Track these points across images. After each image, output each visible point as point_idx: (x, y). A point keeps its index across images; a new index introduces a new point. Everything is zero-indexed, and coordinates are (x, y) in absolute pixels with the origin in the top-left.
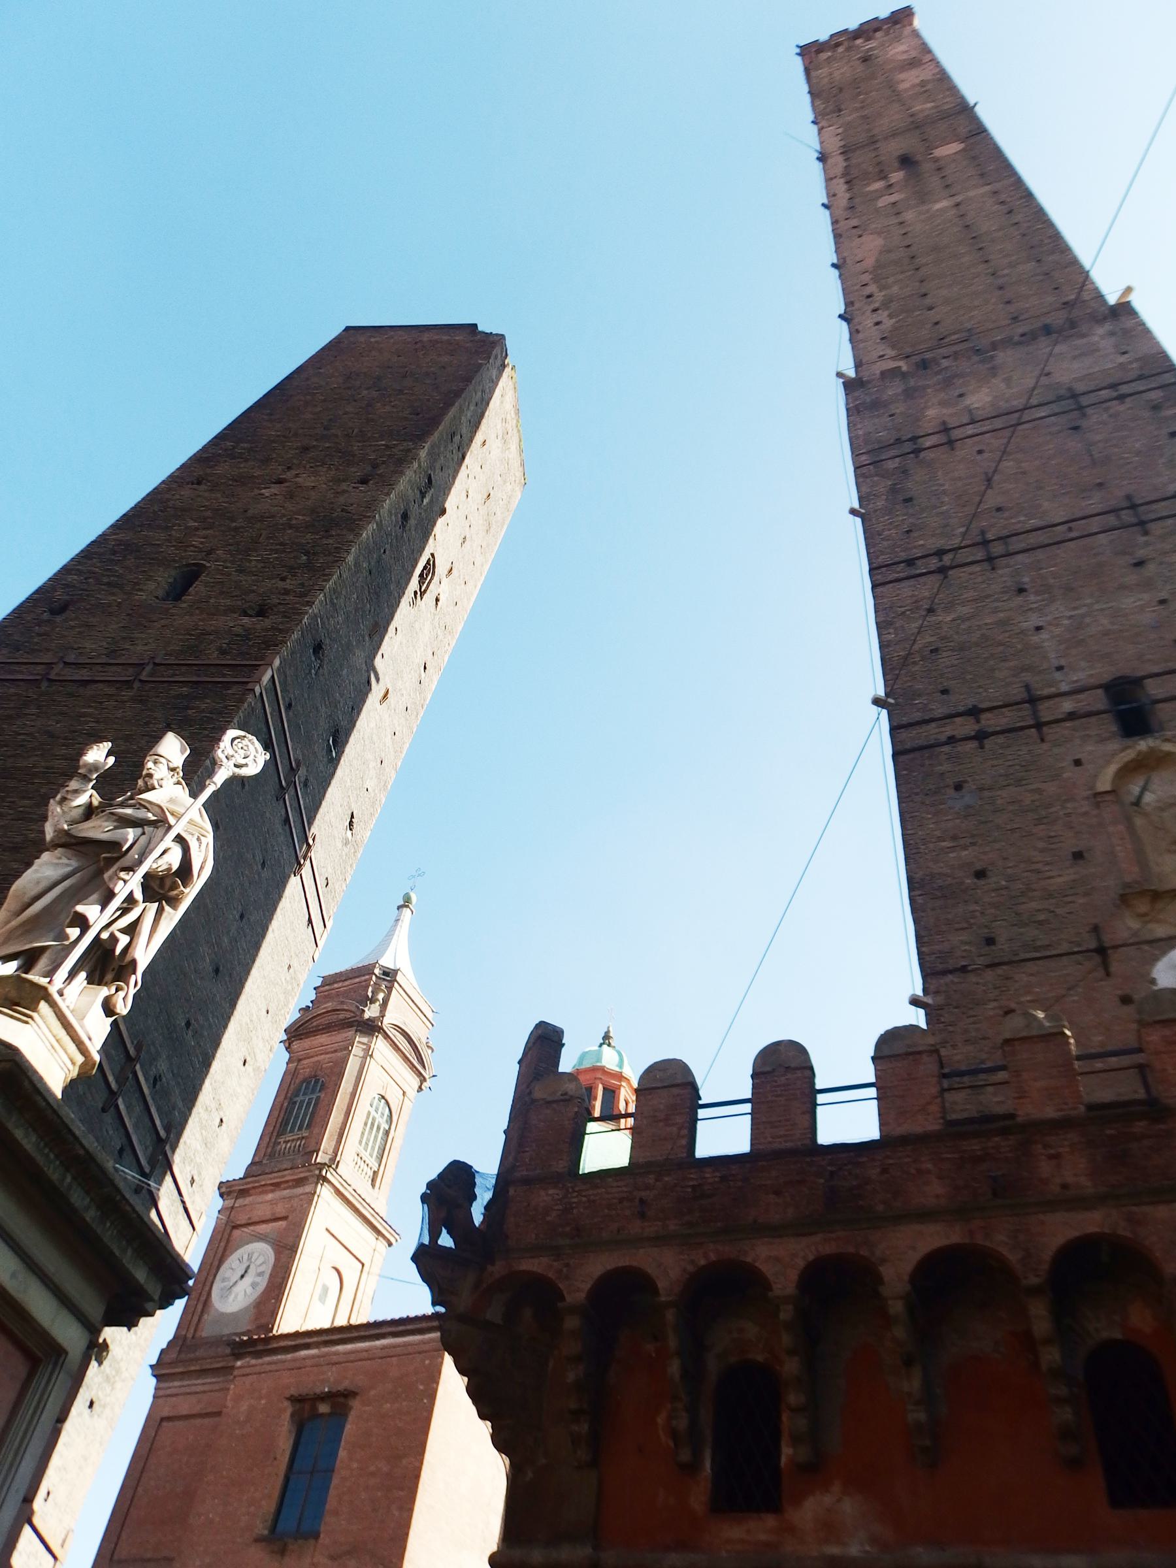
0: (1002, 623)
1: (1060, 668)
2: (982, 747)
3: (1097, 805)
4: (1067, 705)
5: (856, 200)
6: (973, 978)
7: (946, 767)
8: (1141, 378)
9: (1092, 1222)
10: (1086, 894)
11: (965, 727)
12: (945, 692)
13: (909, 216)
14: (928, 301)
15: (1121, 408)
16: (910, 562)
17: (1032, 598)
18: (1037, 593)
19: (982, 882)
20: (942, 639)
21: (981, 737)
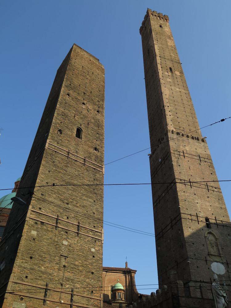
0: (193, 199)
3: (205, 238)
4: (201, 219)
6: (193, 260)
10: (204, 251)
13: (173, 88)
16: (181, 180)
19: (193, 245)
20: (186, 198)
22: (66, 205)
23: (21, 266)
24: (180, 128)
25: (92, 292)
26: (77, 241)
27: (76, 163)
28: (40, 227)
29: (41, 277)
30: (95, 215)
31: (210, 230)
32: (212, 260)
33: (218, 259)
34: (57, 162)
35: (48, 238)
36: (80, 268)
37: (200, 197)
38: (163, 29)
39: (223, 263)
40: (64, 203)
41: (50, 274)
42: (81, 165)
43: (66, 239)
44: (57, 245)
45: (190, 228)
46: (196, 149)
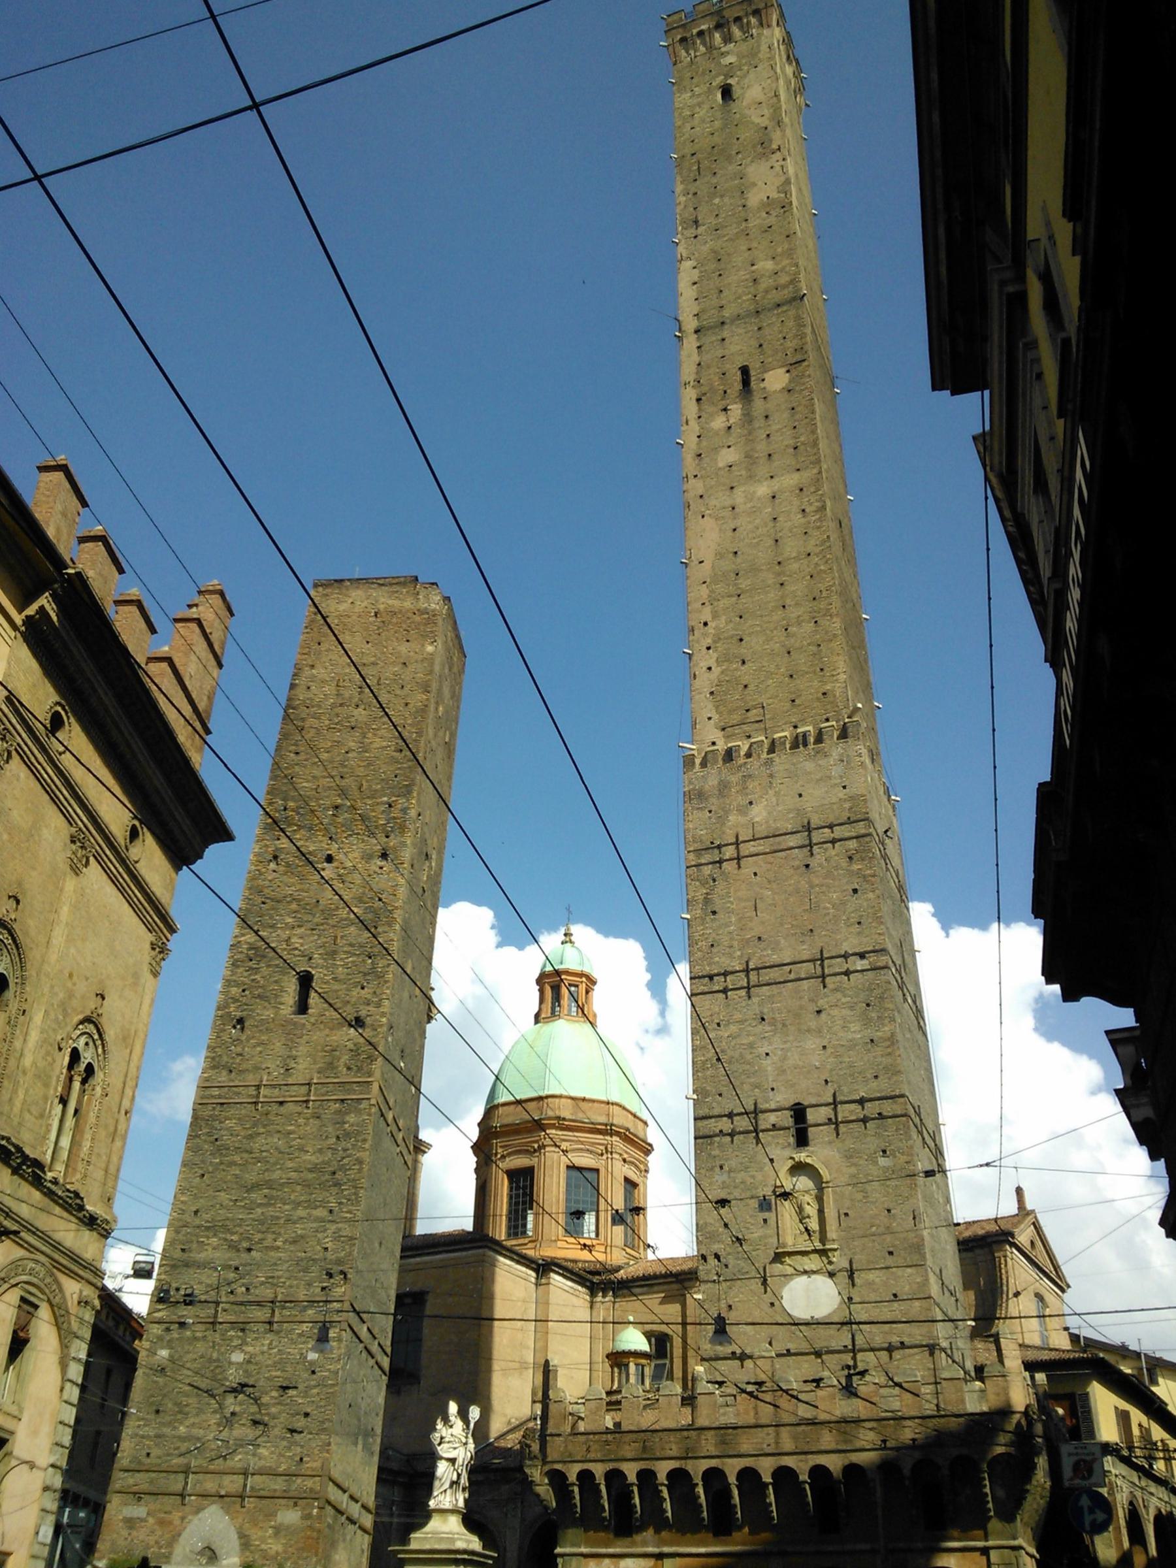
0: (751, 1046)
1: (773, 1089)
2: (732, 1141)
4: (772, 1118)
5: (704, 443)
7: (716, 1152)
8: (849, 822)
9: (713, 1463)
11: (725, 1125)
12: (720, 1095)
14: (743, 651)
15: (833, 853)
16: (711, 977)
17: (768, 1028)
18: (770, 1024)
21: (732, 1135)
22: (244, 1255)
23: (137, 1435)
24: (749, 714)
25: (301, 1459)
26: (270, 1344)
27: (282, 1110)
28: (175, 1335)
29: (178, 1448)
30: (329, 1255)
31: (802, 1156)
32: (790, 1270)
33: (813, 1262)
34: (226, 1139)
35: (195, 1356)
36: (273, 1410)
37: (784, 1025)
38: (734, 107)
39: (831, 1275)
40: (238, 1251)
41: (198, 1439)
42: (299, 1109)
43: (239, 1347)
44: (217, 1367)
45: (721, 1167)
46: (800, 795)
